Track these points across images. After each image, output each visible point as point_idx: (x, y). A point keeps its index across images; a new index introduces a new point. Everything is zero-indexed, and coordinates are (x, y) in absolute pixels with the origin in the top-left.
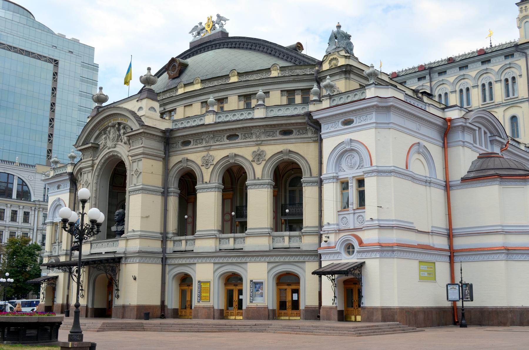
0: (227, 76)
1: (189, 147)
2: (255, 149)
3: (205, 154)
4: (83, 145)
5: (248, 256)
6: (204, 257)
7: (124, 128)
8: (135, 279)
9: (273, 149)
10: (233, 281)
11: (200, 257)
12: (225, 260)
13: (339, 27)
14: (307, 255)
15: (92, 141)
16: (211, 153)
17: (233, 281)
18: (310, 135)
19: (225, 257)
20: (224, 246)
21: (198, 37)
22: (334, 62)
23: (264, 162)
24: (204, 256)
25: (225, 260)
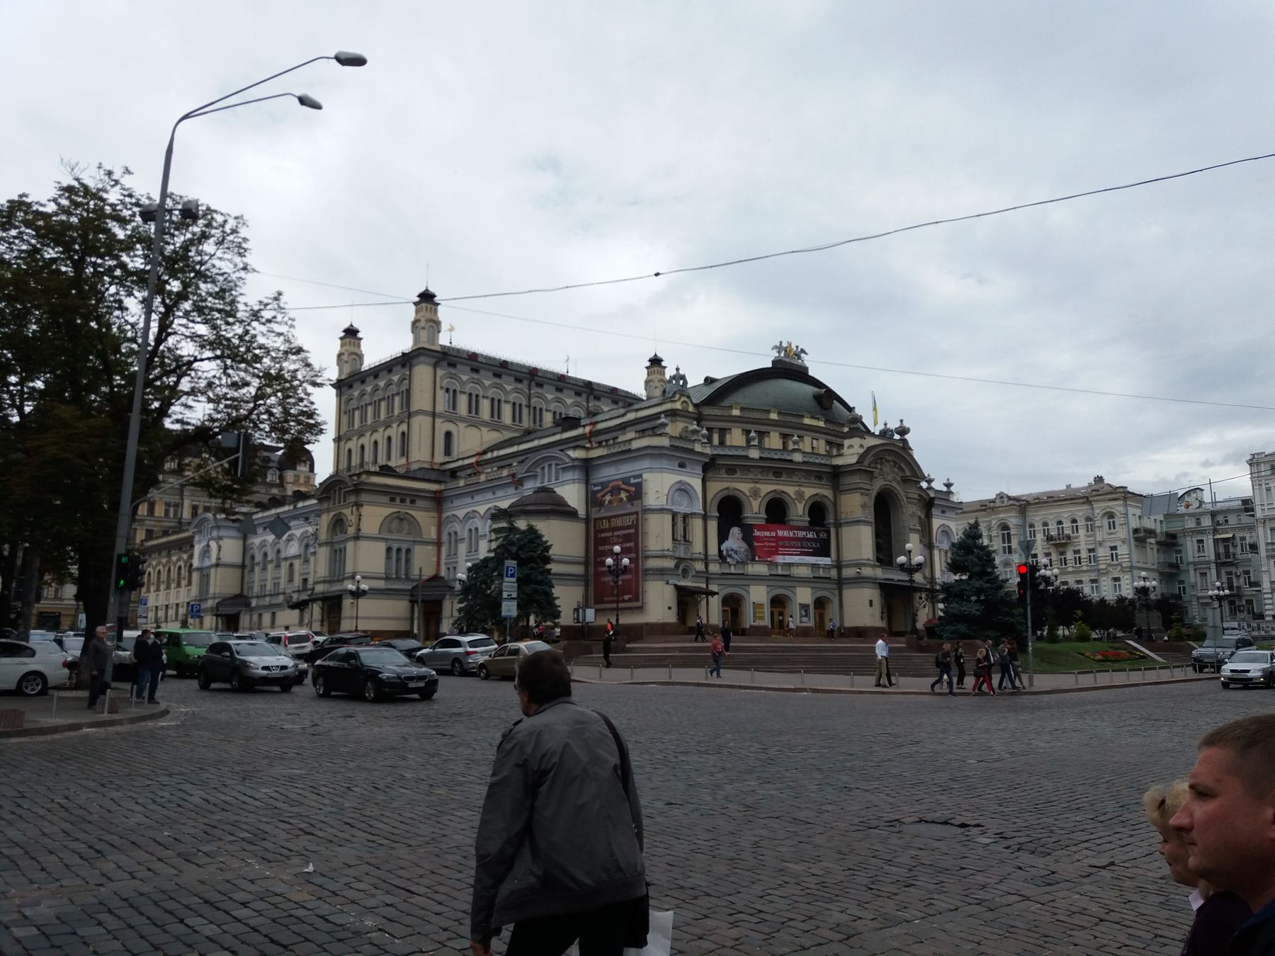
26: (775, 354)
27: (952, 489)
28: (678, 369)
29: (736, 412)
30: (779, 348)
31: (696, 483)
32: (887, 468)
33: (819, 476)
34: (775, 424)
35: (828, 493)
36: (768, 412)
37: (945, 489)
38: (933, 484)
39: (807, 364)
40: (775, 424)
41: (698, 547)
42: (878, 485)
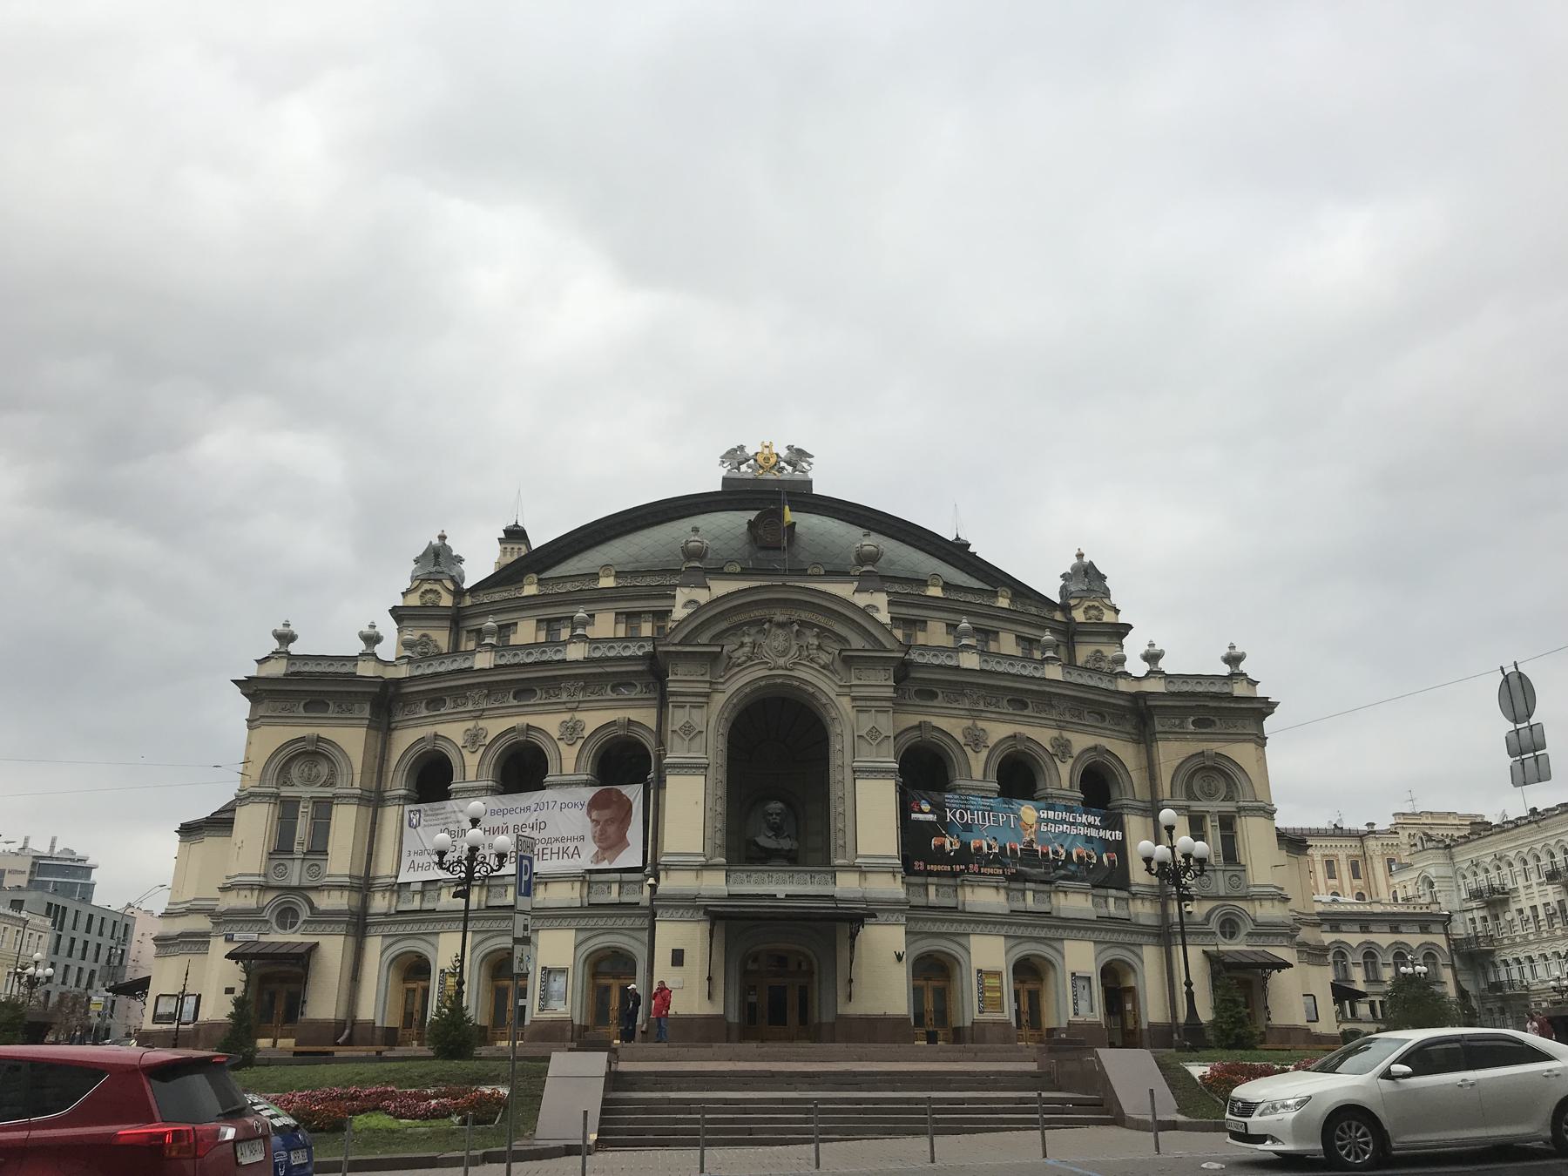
0: (924, 583)
1: (935, 703)
2: (1055, 733)
3: (969, 723)
4: (680, 644)
5: (1065, 928)
6: (987, 923)
7: (818, 636)
8: (899, 958)
9: (1080, 741)
10: (1030, 972)
11: (978, 923)
12: (1027, 932)
13: (1080, 556)
14: (1143, 934)
15: (704, 639)
16: (981, 724)
17: (1030, 972)
18: (1129, 728)
19: (1027, 925)
20: (1019, 906)
21: (735, 474)
22: (1093, 612)
23: (1071, 761)
24: (986, 921)
25: (1027, 932)
26: (723, 472)
27: (1243, 667)
28: (442, 537)
29: (530, 589)
30: (735, 456)
31: (351, 739)
32: (778, 640)
33: (620, 682)
34: (605, 597)
35: (646, 716)
36: (595, 576)
37: (1225, 670)
38: (1165, 665)
39: (810, 475)
40: (605, 597)
41: (340, 860)
42: (737, 683)
